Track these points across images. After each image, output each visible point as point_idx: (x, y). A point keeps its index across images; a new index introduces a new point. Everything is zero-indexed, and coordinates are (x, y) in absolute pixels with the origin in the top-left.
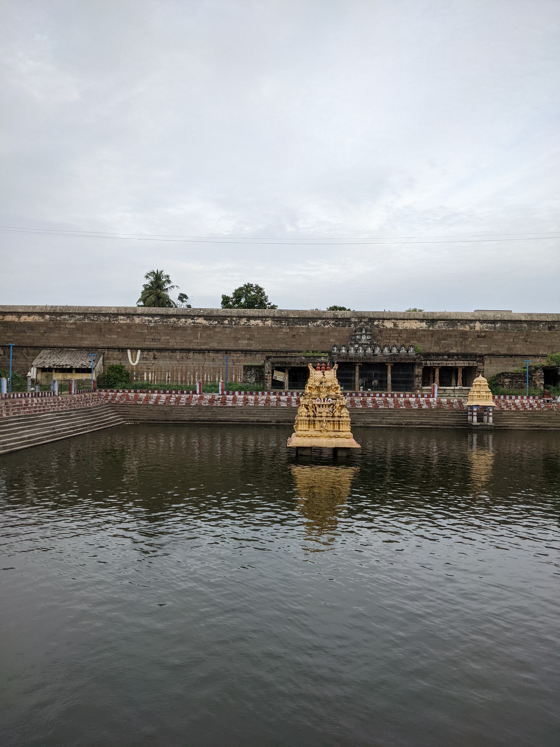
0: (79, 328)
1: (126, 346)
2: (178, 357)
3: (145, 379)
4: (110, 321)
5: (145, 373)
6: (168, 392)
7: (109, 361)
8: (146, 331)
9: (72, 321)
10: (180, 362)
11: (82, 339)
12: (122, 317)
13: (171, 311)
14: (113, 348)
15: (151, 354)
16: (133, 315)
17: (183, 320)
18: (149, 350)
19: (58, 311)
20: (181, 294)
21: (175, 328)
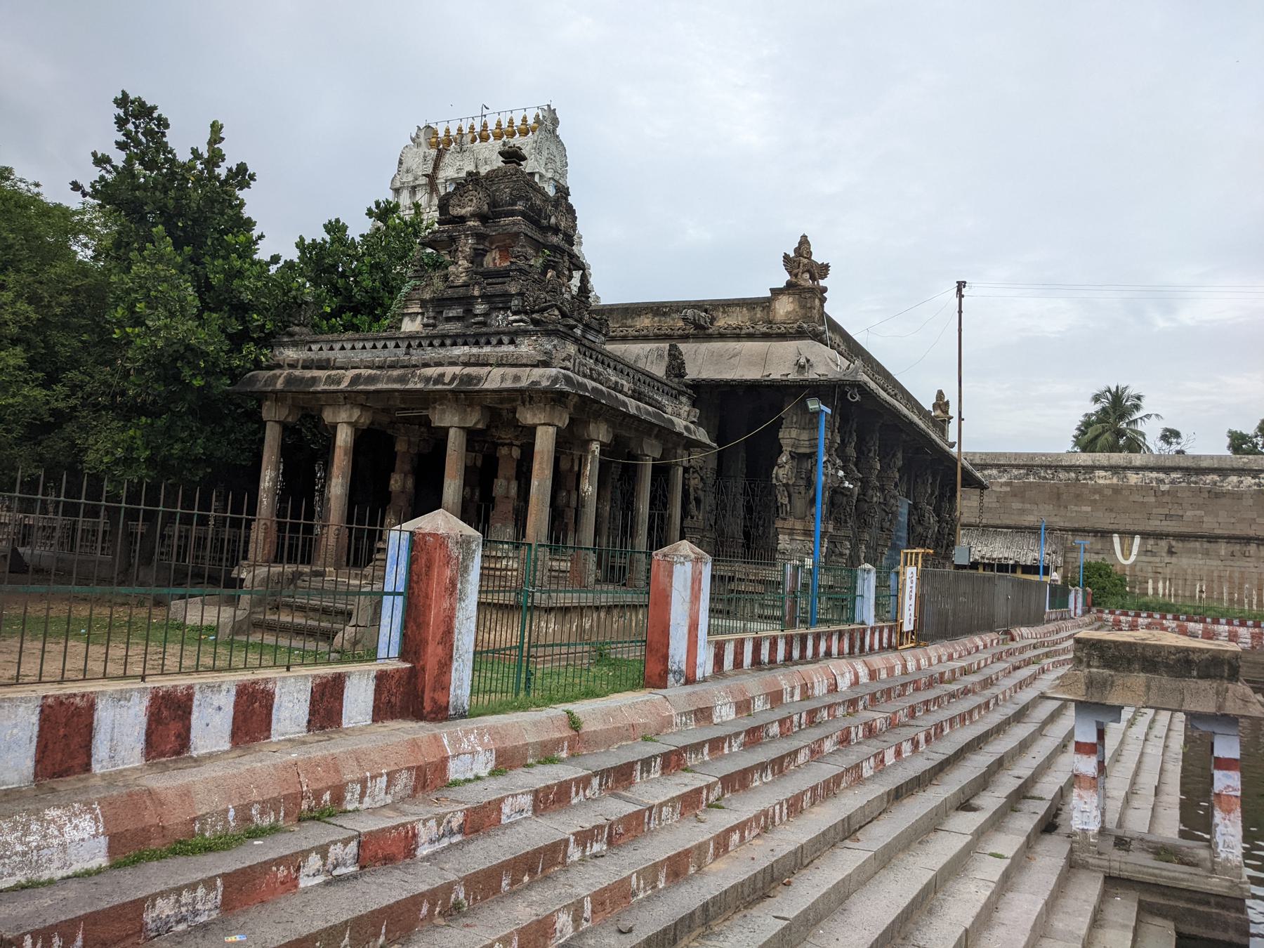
0: (1018, 492)
1: (1111, 527)
2: (1223, 553)
3: (1150, 591)
4: (1077, 479)
5: (1150, 581)
6: (1250, 623)
7: (1075, 555)
8: (1153, 499)
9: (1003, 480)
10: (1228, 563)
11: (1022, 512)
12: (1102, 473)
13: (1137, 459)
14: (1084, 531)
15: (1163, 544)
16: (1125, 468)
17: (1234, 479)
18: (1159, 536)
19: (977, 461)
20: (1167, 430)
21: (1216, 495)
